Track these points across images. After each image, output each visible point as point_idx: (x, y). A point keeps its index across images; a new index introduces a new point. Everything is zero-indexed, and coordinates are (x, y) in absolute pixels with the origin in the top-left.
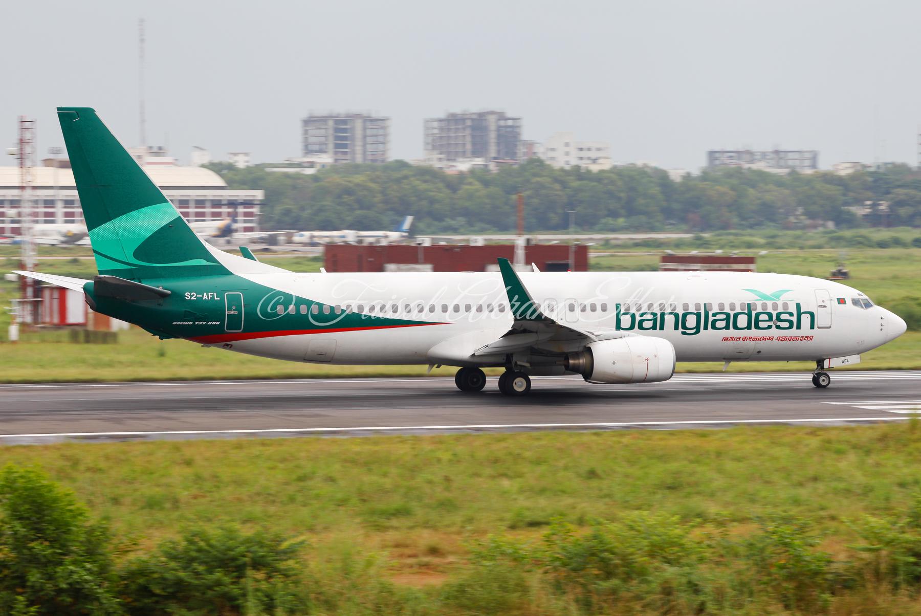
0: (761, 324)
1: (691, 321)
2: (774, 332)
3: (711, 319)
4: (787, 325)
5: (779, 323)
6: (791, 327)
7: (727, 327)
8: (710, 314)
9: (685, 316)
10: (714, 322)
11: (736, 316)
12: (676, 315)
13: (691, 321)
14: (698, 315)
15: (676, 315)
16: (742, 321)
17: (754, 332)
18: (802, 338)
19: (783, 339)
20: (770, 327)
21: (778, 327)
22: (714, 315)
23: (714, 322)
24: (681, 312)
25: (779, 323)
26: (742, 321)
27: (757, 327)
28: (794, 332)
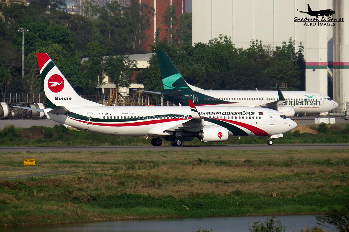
0: (309, 104)
1: (293, 103)
2: (311, 106)
3: (297, 102)
4: (314, 104)
5: (312, 104)
6: (315, 105)
7: (301, 105)
8: (297, 101)
9: (292, 101)
10: (298, 103)
11: (303, 101)
12: (290, 101)
13: (293, 103)
14: (295, 101)
15: (290, 101)
16: (304, 103)
17: (307, 106)
18: (317, 108)
19: (313, 108)
20: (310, 105)
21: (312, 105)
22: (298, 101)
23: (298, 103)
24: (291, 100)
25: (312, 104)
26: (304, 103)
27: (307, 105)
28: (315, 106)
